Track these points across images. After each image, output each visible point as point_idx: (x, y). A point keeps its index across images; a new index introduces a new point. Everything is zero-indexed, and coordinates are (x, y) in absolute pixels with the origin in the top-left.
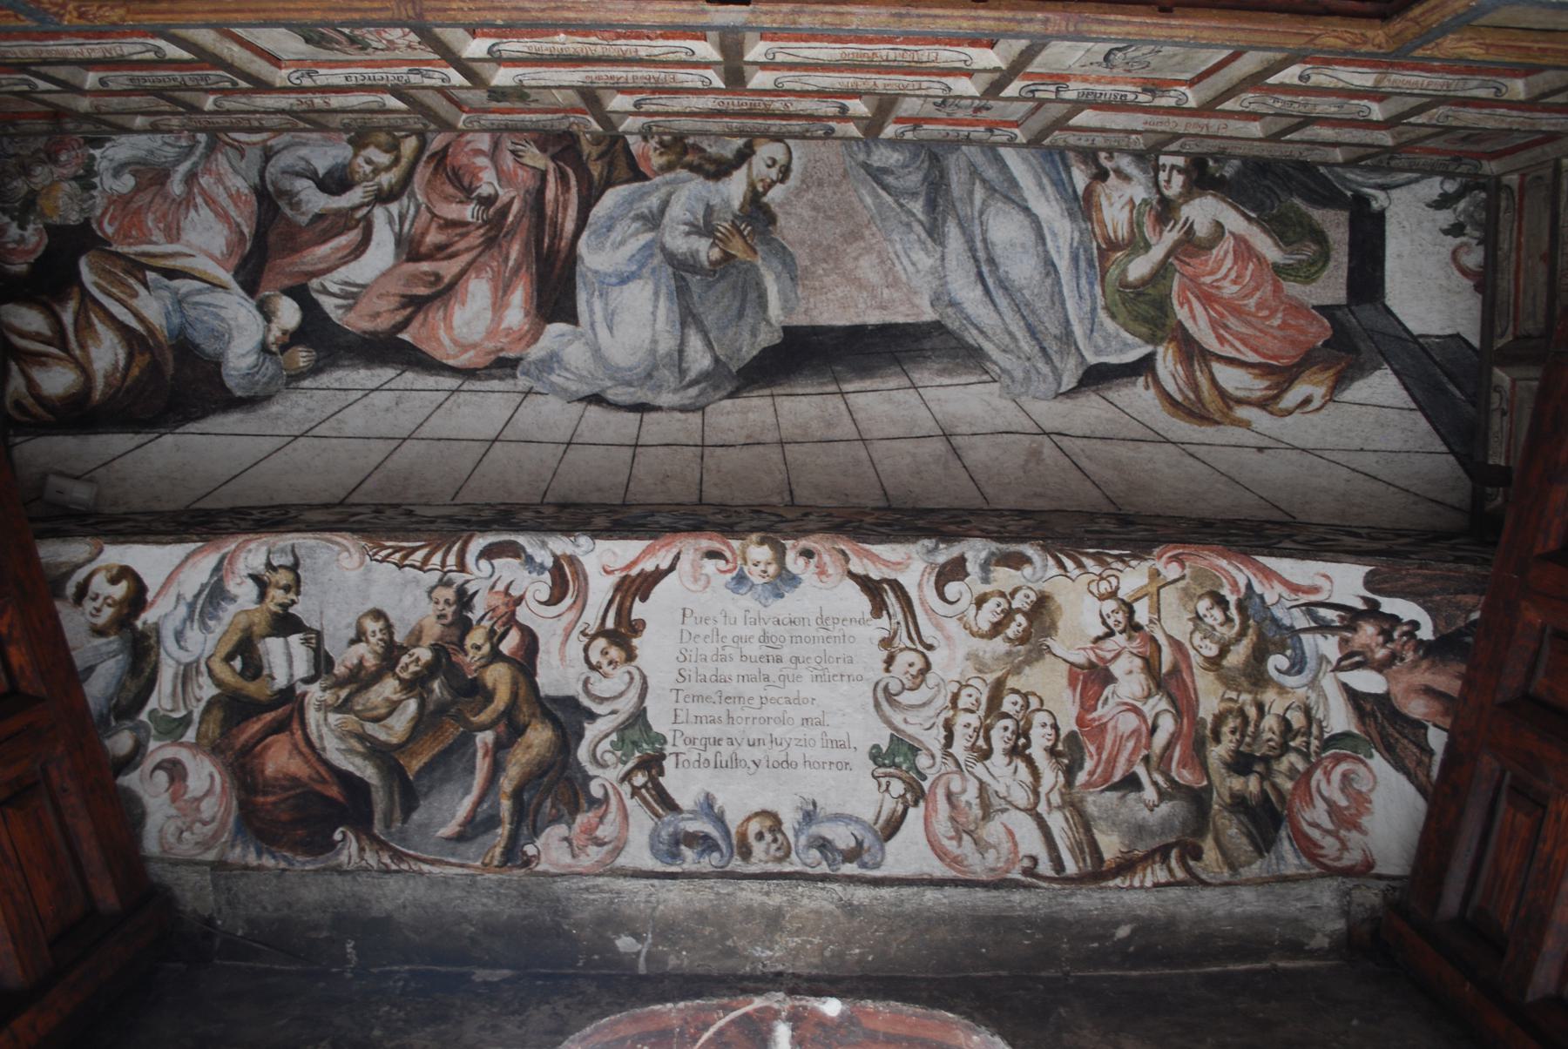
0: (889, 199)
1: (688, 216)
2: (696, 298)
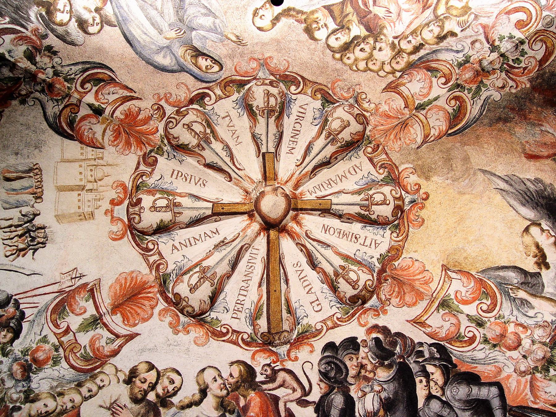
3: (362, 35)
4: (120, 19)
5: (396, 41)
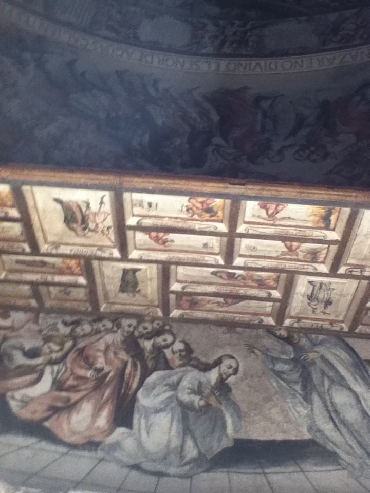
0: (284, 384)
1: (190, 386)
2: (191, 422)
3: (143, 339)
4: (361, 367)
5: (115, 329)
